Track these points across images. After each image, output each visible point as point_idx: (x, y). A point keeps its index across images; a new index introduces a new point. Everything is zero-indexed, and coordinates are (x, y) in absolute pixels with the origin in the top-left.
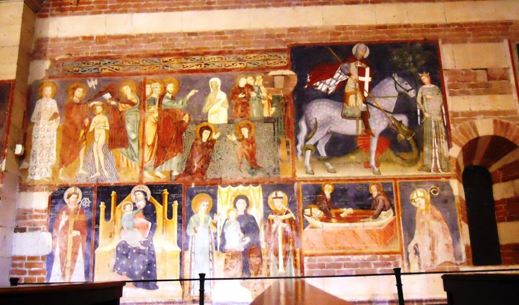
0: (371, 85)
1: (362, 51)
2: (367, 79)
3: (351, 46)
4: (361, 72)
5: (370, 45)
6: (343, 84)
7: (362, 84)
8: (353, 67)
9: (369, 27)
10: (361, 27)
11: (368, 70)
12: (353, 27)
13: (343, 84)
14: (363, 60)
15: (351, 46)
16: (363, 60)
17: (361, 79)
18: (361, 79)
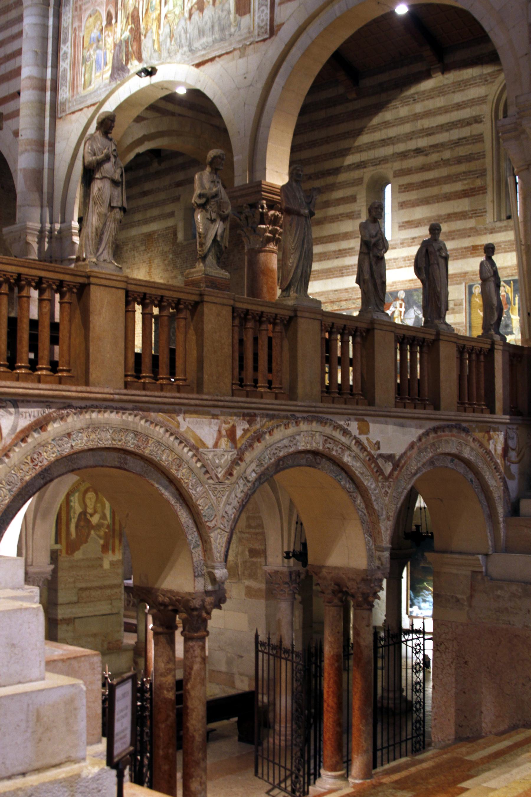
0: (405, 313)
1: (402, 295)
2: (403, 310)
3: (397, 292)
4: (401, 306)
5: (406, 291)
6: (394, 312)
7: (401, 312)
8: (398, 303)
9: (406, 281)
10: (403, 281)
11: (403, 305)
12: (399, 282)
13: (394, 312)
14: (402, 300)
15: (397, 292)
16: (402, 300)
17: (401, 309)
18: (401, 309)
